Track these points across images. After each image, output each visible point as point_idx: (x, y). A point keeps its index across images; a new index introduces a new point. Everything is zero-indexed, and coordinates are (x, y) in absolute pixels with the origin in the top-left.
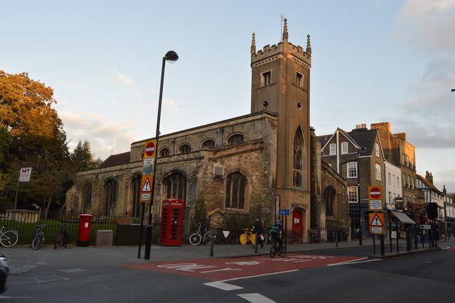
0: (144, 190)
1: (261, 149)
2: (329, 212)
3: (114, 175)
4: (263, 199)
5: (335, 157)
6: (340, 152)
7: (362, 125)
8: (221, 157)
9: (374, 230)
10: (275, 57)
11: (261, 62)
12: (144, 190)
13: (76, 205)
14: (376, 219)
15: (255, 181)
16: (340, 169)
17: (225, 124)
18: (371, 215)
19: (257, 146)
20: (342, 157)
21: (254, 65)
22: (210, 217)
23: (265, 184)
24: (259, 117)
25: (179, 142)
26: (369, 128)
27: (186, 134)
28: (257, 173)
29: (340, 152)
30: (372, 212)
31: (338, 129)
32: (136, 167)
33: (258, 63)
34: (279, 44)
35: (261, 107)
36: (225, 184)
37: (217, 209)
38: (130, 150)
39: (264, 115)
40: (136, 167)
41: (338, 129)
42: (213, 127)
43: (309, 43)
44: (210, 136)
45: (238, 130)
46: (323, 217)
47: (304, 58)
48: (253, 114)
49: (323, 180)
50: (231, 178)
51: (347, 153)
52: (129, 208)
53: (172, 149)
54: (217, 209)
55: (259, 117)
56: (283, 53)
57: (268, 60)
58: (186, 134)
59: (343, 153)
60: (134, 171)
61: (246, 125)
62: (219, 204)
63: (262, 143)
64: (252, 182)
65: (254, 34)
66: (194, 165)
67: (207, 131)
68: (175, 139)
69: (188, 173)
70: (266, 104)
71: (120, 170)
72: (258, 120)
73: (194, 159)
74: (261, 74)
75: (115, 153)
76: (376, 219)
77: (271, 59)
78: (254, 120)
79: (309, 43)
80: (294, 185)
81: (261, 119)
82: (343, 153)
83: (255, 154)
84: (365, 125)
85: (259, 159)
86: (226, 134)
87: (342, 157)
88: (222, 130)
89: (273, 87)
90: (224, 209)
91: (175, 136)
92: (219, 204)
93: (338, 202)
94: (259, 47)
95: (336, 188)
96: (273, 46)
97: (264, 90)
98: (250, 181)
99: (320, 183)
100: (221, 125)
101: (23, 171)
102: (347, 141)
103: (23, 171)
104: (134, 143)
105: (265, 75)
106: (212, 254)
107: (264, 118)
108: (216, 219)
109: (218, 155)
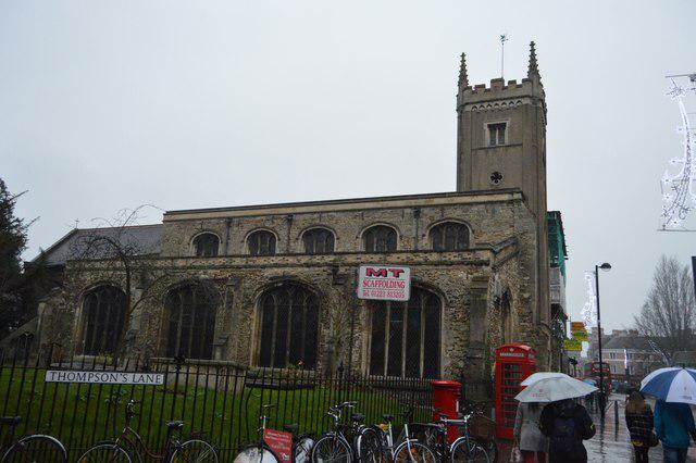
1: (515, 255)
9: (622, 398)
11: (485, 105)
13: (67, 332)
17: (422, 202)
19: (511, 250)
21: (469, 108)
23: (521, 316)
24: (506, 197)
25: (301, 222)
27: (321, 208)
32: (277, 266)
34: (524, 81)
35: (485, 182)
39: (517, 196)
40: (277, 266)
42: (385, 204)
44: (387, 218)
48: (459, 194)
52: (254, 347)
53: (283, 233)
55: (506, 197)
57: (500, 103)
58: (321, 208)
60: (268, 273)
61: (475, 208)
63: (516, 243)
67: (379, 209)
68: (291, 215)
69: (445, 289)
70: (496, 177)
71: (224, 267)
72: (502, 202)
77: (508, 102)
78: (491, 203)
81: (511, 202)
83: (514, 263)
86: (426, 221)
88: (417, 211)
89: (512, 150)
91: (290, 210)
96: (510, 82)
97: (490, 152)
101: (370, 273)
103: (370, 273)
104: (168, 213)
105: (489, 126)
107: (518, 201)
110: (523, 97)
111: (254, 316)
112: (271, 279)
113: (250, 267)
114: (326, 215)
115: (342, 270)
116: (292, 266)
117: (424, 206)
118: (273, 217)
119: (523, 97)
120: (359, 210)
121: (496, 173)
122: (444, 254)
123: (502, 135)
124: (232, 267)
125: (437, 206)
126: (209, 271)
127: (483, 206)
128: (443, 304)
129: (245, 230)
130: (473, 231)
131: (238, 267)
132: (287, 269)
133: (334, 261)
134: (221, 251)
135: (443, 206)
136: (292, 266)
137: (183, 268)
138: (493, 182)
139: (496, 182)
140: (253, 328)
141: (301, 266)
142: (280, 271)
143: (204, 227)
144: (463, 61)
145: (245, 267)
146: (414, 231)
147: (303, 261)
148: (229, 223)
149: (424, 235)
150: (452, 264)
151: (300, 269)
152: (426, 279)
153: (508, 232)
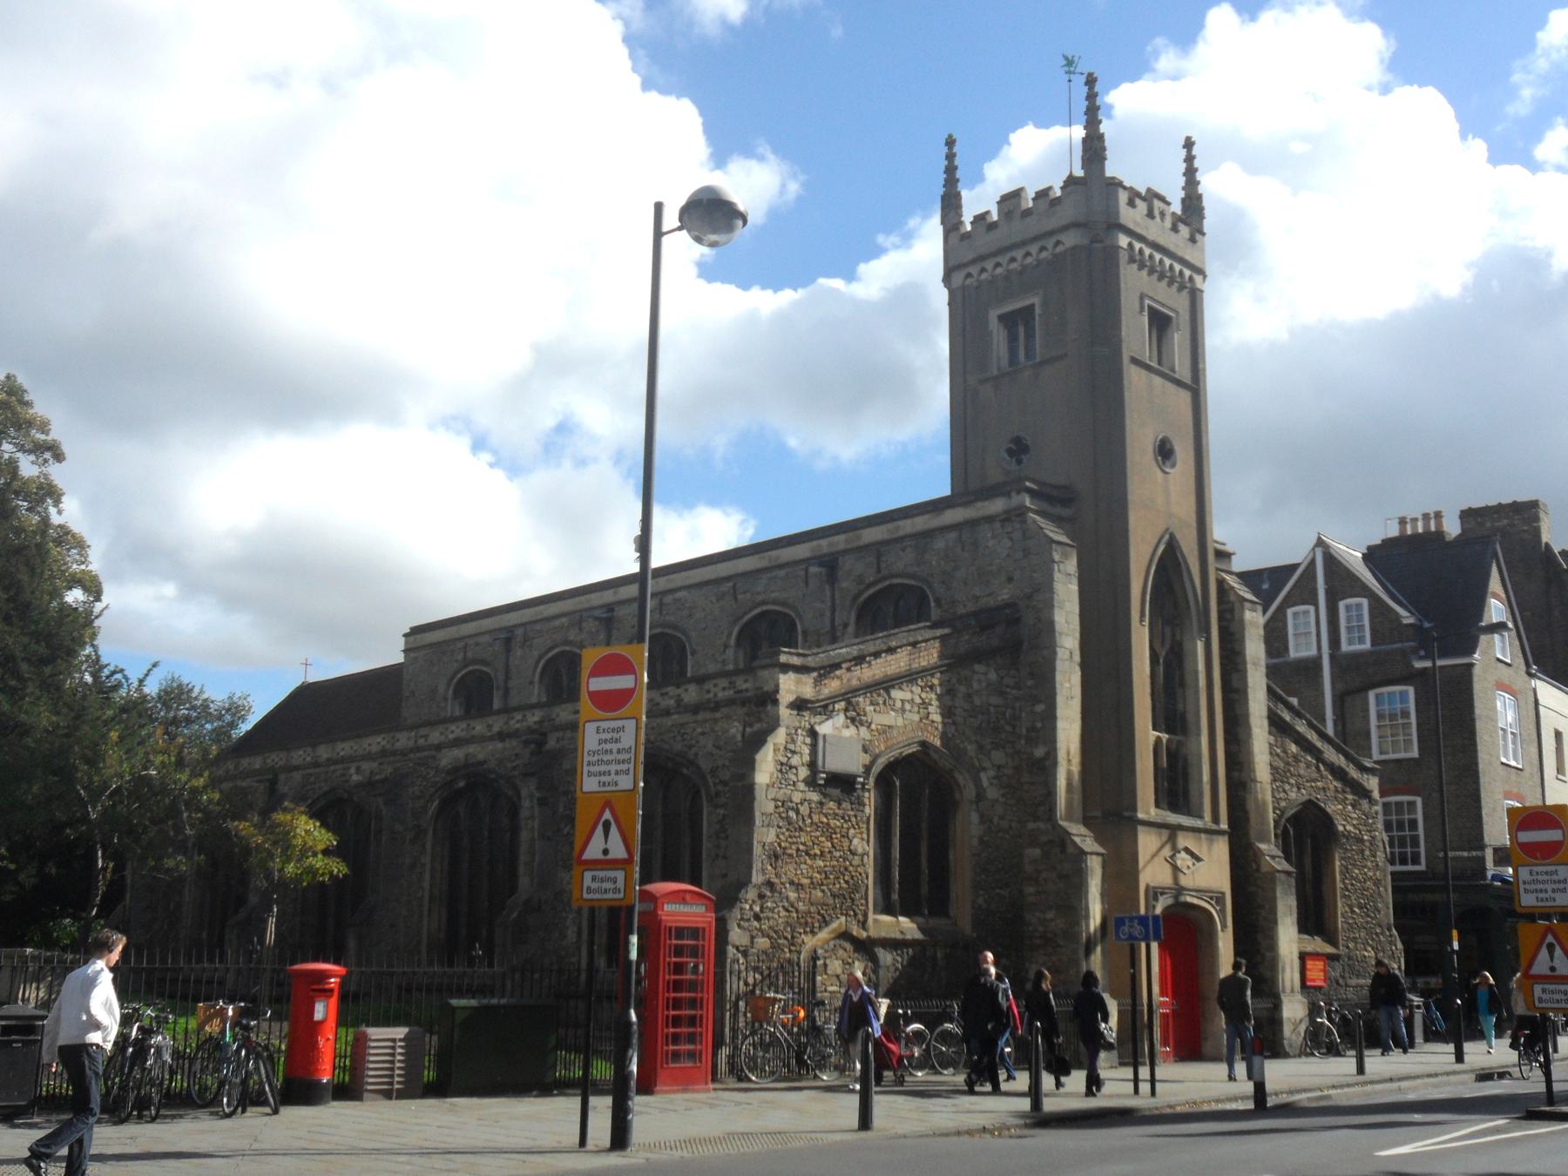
0: (593, 851)
2: (1314, 920)
3: (355, 778)
4: (1028, 868)
5: (1312, 666)
6: (1335, 642)
7: (1426, 517)
8: (848, 697)
10: (1050, 243)
12: (593, 851)
14: (1551, 948)
15: (992, 793)
16: (1340, 718)
17: (840, 541)
18: (1526, 932)
20: (1345, 666)
22: (814, 958)
26: (1452, 528)
28: (998, 756)
29: (1335, 642)
30: (1531, 917)
31: (1320, 543)
32: (457, 743)
33: (974, 270)
36: (869, 810)
37: (839, 923)
38: (399, 658)
40: (457, 743)
41: (1320, 543)
43: (1190, 173)
45: (901, 561)
46: (1289, 940)
47: (1177, 241)
49: (1278, 775)
50: (891, 785)
51: (1367, 646)
54: (839, 923)
55: (997, 506)
56: (1076, 225)
57: (1019, 254)
59: (1345, 647)
60: (448, 758)
61: (939, 544)
62: (847, 900)
63: (1015, 621)
64: (980, 796)
65: (950, 142)
66: (735, 729)
68: (610, 608)
69: (705, 765)
71: (384, 753)
72: (990, 519)
73: (730, 702)
74: (993, 315)
75: (312, 679)
76: (1551, 948)
78: (972, 523)
79: (1190, 173)
80: (1157, 805)
82: (1345, 647)
84: (1438, 515)
85: (1002, 694)
87: (1345, 666)
88: (830, 564)
90: (870, 921)
92: (847, 900)
93: (1346, 871)
94: (978, 201)
95: (1332, 808)
98: (970, 792)
99: (1268, 789)
100: (824, 545)
102: (1365, 591)
104: (416, 631)
105: (1008, 320)
106: (865, 1122)
108: (835, 966)
109: (833, 686)
110: (1065, 228)
111: (427, 859)
112: (449, 772)
113: (418, 749)
114: (668, 599)
115: (552, 743)
116: (482, 739)
117: (845, 552)
118: (578, 618)
119: (1065, 228)
120: (728, 578)
121: (1018, 441)
122: (709, 685)
123: (1030, 335)
124: (394, 753)
125: (867, 547)
126: (367, 766)
127: (953, 535)
128: (704, 798)
129: (536, 653)
130: (938, 601)
131: (403, 753)
132: (472, 749)
133: (540, 722)
134: (497, 705)
135: (878, 549)
136: (482, 739)
137: (330, 761)
138: (1014, 467)
139: (1019, 462)
140: (426, 885)
141: (491, 738)
142: (458, 754)
143: (470, 655)
144: (950, 157)
145: (412, 750)
146: (828, 614)
147: (496, 729)
148: (508, 641)
149: (846, 626)
150: (717, 706)
151: (490, 747)
152: (678, 747)
153: (1004, 595)
